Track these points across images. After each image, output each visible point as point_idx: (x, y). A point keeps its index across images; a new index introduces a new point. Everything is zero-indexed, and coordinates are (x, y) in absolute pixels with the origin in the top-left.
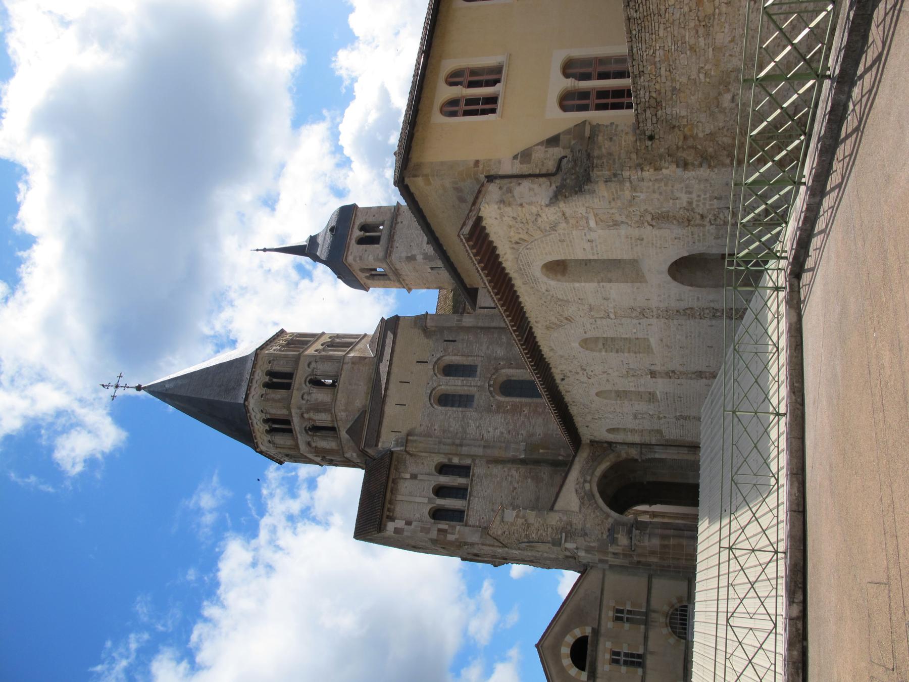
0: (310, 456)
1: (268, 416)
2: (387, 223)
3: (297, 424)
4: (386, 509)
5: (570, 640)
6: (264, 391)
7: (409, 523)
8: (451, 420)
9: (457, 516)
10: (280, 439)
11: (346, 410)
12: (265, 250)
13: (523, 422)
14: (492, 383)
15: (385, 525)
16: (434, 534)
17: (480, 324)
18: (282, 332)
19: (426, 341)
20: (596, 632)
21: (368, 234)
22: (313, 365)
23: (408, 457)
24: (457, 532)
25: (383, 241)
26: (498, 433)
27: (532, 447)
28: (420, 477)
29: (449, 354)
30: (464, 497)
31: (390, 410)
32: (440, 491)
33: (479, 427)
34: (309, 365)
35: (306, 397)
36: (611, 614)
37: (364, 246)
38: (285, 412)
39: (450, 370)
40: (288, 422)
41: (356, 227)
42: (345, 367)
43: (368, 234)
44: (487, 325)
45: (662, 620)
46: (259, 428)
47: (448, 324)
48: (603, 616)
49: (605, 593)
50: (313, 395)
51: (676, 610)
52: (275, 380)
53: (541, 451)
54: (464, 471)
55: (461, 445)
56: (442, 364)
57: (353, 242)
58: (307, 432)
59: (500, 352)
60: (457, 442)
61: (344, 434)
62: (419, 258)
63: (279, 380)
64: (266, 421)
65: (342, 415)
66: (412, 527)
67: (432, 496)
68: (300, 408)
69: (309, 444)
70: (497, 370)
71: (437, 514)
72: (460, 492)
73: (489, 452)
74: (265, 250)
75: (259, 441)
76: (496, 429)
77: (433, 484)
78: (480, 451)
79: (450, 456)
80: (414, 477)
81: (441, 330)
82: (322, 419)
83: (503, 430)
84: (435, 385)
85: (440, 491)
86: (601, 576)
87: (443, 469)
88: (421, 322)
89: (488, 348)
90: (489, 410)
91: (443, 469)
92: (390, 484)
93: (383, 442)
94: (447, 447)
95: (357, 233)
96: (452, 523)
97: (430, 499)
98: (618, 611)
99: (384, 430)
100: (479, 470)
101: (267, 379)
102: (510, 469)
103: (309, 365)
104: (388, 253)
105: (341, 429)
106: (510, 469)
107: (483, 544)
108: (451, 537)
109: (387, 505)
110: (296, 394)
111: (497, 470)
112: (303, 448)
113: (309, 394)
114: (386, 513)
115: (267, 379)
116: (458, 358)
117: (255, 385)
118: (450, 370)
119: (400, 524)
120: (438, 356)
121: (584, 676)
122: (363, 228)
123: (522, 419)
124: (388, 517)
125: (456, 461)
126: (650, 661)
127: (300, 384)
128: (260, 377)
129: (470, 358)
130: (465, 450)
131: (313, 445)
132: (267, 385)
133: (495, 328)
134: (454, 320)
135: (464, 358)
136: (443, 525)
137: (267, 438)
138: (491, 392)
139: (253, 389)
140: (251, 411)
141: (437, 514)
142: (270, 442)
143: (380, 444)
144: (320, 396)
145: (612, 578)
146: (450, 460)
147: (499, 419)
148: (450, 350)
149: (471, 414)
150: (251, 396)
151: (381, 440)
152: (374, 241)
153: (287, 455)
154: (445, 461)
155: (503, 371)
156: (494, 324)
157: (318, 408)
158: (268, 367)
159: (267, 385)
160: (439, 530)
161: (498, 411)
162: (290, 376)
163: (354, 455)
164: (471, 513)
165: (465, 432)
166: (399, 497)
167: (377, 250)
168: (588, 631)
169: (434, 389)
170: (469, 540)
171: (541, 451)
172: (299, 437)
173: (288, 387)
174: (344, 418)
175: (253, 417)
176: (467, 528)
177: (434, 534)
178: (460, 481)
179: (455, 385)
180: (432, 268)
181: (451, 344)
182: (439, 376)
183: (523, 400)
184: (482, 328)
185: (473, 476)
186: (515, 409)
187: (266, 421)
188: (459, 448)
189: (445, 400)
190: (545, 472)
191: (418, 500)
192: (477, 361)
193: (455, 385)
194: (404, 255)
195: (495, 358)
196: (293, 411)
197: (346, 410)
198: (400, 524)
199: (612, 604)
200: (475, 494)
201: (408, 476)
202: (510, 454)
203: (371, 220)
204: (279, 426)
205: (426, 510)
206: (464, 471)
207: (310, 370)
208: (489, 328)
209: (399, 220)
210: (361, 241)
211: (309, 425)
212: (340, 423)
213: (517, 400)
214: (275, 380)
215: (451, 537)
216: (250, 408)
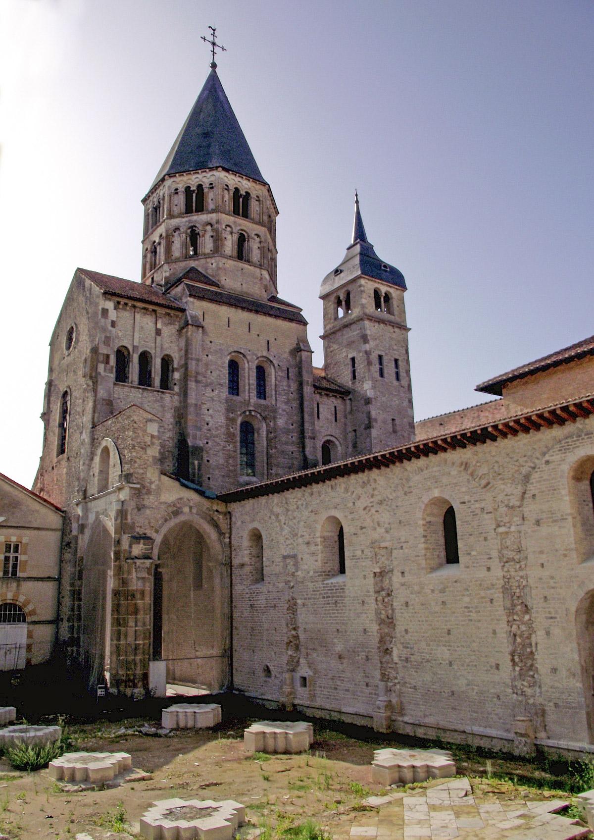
0: (161, 230)
1: (206, 190)
2: (391, 318)
3: (200, 218)
4: (126, 301)
6: (232, 188)
7: (113, 324)
8: (218, 372)
9: (121, 376)
10: (181, 199)
11: (219, 268)
12: (357, 202)
13: (219, 444)
14: (253, 413)
15: (110, 300)
16: (104, 350)
17: (306, 404)
18: (277, 213)
19: (287, 350)
21: (382, 299)
22: (258, 240)
23: (177, 327)
24: (107, 374)
26: (208, 419)
27: (198, 450)
28: (159, 338)
29: (276, 372)
30: (141, 382)
31: (225, 311)
32: (145, 358)
33: (213, 400)
34: (258, 236)
35: (228, 229)
36: (14, 539)
37: (373, 295)
38: (211, 206)
39: (261, 372)
40: (200, 209)
41: (389, 289)
42: (258, 270)
43: (382, 299)
44: (305, 409)
45: (10, 596)
46: (193, 180)
47: (304, 373)
48: (11, 531)
49: (36, 532)
50: (229, 237)
51: (20, 609)
52: (241, 200)
53: (196, 462)
54: (165, 384)
55: (197, 382)
56: (266, 366)
57: (376, 285)
58: (192, 227)
59: (281, 422)
60: (200, 378)
61: (193, 264)
62: (367, 347)
63: (241, 204)
64: (200, 187)
66: (110, 328)
67: (141, 350)
68: (218, 222)
69: (177, 229)
70: (264, 418)
71: (122, 356)
72: (145, 380)
73: (191, 409)
74: (357, 202)
75: (178, 179)
76: (212, 417)
77: (152, 352)
78: (192, 400)
79: (182, 370)
80: (158, 332)
81: (299, 366)
82: (207, 244)
83: (210, 424)
84: (249, 357)
85: (145, 358)
86: (53, 527)
87: (166, 362)
88: (301, 348)
89: (284, 410)
90: (230, 409)
91: (166, 362)
92: (151, 307)
93: (193, 303)
94: (194, 368)
95: (384, 289)
96: (114, 370)
97: (137, 347)
98: (16, 547)
99: (205, 304)
100: (170, 400)
101: (243, 193)
102: (170, 430)
103: (258, 236)
104: (370, 318)
105: (197, 262)
106: (170, 430)
107: (95, 401)
108: (101, 367)
109: (130, 303)
110: (230, 219)
111: (169, 417)
112: (175, 222)
113: (231, 233)
114: (123, 301)
115: (243, 193)
116: (273, 381)
117: (237, 179)
118: (261, 372)
119: (113, 315)
120: (275, 362)
122: (387, 298)
123: (222, 444)
124: (119, 303)
125: (177, 375)
127: (240, 225)
128: (245, 185)
129: (273, 393)
130: (192, 385)
131: (176, 234)
132: (237, 190)
133: (303, 418)
134: (306, 377)
135: (273, 387)
137: (181, 188)
138: (245, 412)
139: (233, 177)
140: (212, 173)
141: (122, 356)
142: (176, 189)
143: (191, 299)
144: (229, 245)
145: (53, 538)
146: (177, 370)
147: (221, 420)
148: (280, 373)
149: (225, 392)
150: (226, 174)
151: (195, 301)
152: (378, 305)
153: (156, 209)
154: (175, 366)
155: (264, 425)
156: (306, 417)
157: (218, 239)
158: (253, 194)
159: (237, 190)
160: (108, 356)
161: (228, 418)
163: (168, 274)
164: (126, 389)
165: (207, 386)
166: (138, 316)
167: (371, 309)
169: (244, 356)
170: (100, 388)
171: (196, 462)
172: (184, 220)
173: (236, 212)
174: (209, 266)
175: (204, 174)
176: (111, 385)
177: (104, 350)
178: (157, 381)
179: (249, 378)
180: (353, 359)
181: (284, 374)
182: (256, 362)
183: (239, 444)
184: (301, 405)
185: (163, 392)
186: (230, 436)
187: (200, 187)
188: (193, 379)
189: (234, 367)
190: (170, 466)
191: (137, 335)
192: (270, 401)
193: (249, 378)
194: (368, 332)
195: (275, 418)
196: (214, 215)
197: (219, 268)
198: (113, 315)
199: (25, 540)
200: (145, 394)
201: (159, 326)
202: (191, 431)
203: (395, 303)
204: (195, 200)
205: (126, 343)
206: (165, 384)
207: (253, 236)
208: (302, 411)
209: (396, 330)
210: (376, 292)
211: (200, 230)
212: (203, 261)
213: (238, 439)
214: (241, 200)
215: (101, 367)
216: (215, 173)
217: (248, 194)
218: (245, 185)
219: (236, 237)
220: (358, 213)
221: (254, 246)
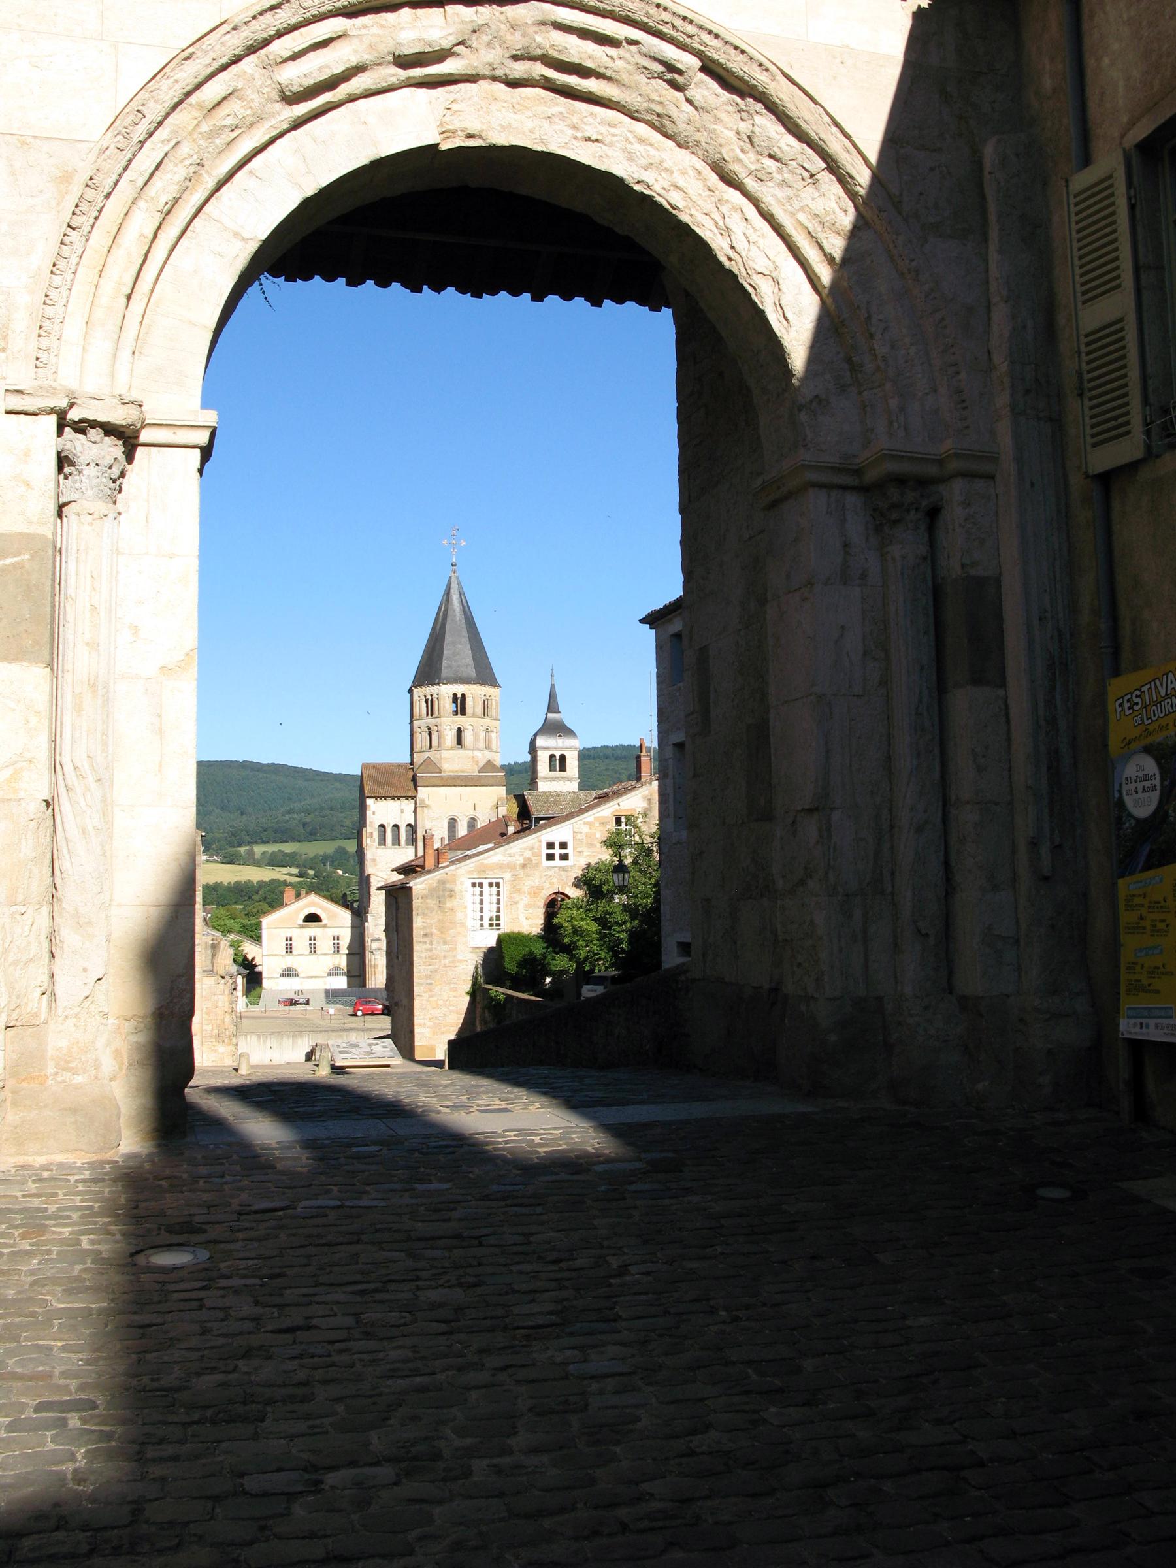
3: (431, 721)
5: (319, 912)
9: (382, 841)
20: (325, 926)
25: (552, 773)
46: (428, 690)
61: (427, 754)
65: (437, 754)
72: (397, 841)
80: (402, 811)
101: (459, 696)
115: (459, 696)
121: (301, 922)
126: (313, 957)
132: (455, 695)
136: (376, 834)
144: (450, 737)
159: (455, 695)
162: (463, 713)
168: (324, 921)
173: (455, 713)
217: (463, 695)
218: (460, 689)
219: (454, 732)
220: (553, 688)
221: (467, 736)
